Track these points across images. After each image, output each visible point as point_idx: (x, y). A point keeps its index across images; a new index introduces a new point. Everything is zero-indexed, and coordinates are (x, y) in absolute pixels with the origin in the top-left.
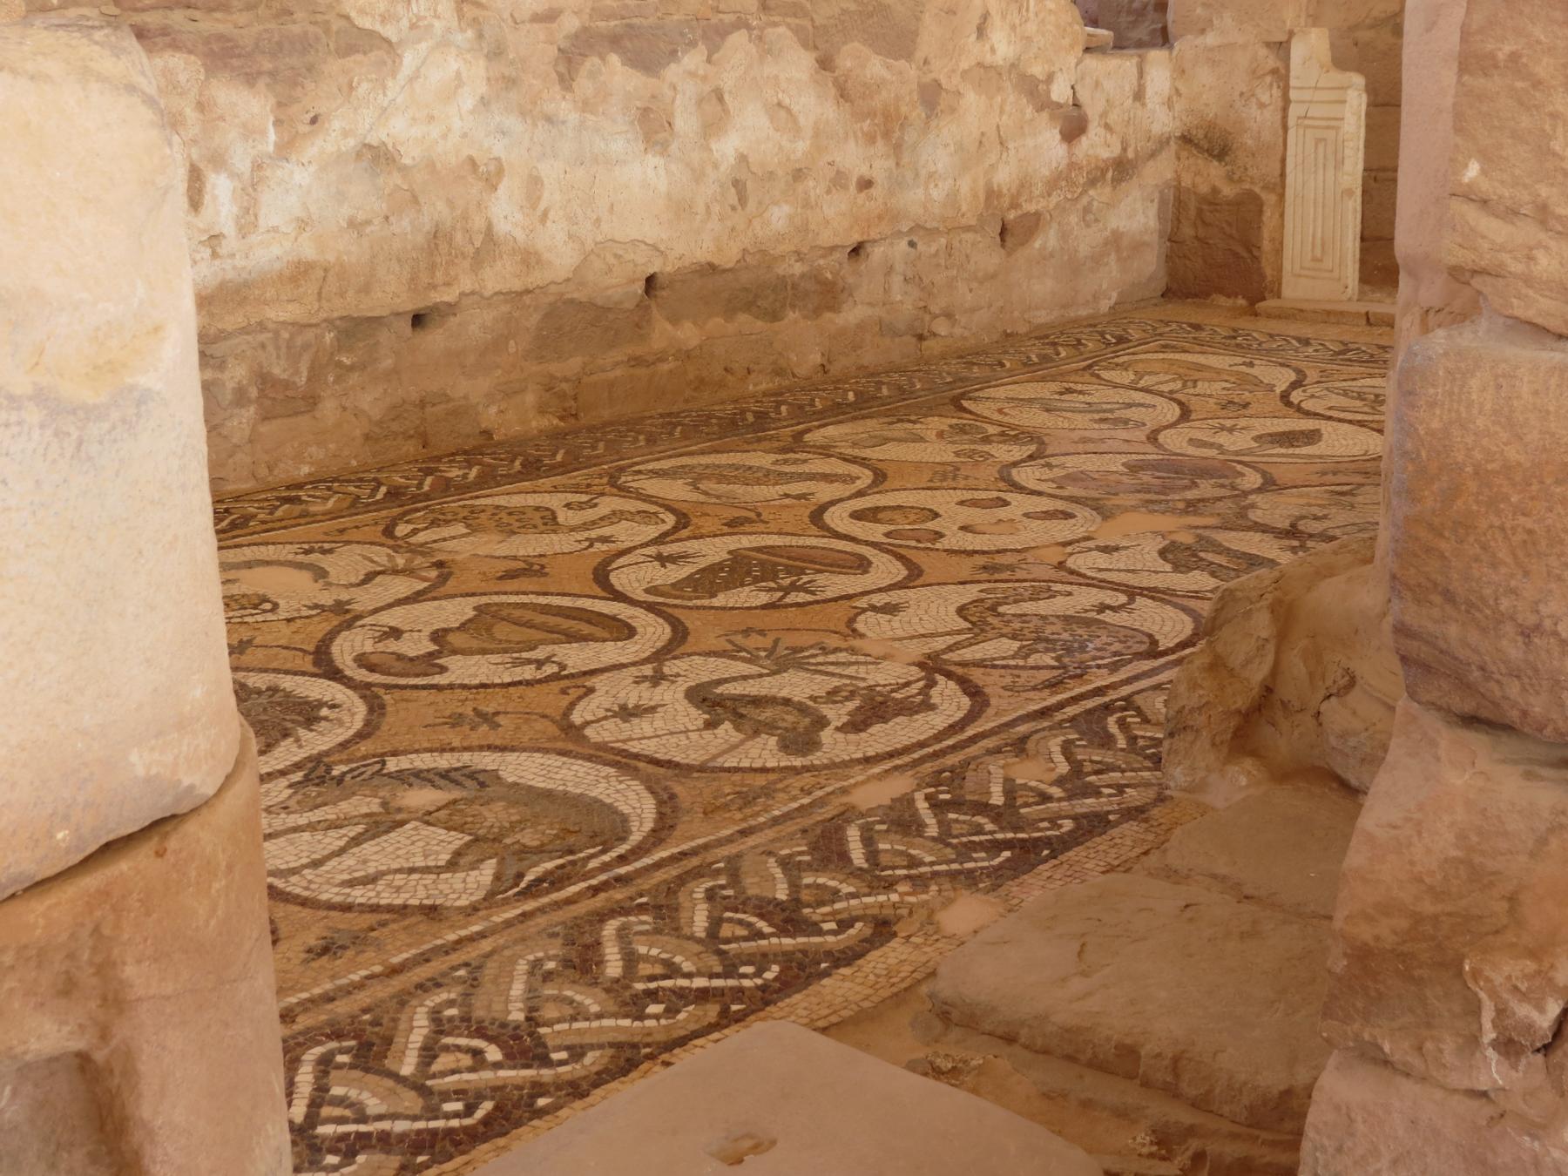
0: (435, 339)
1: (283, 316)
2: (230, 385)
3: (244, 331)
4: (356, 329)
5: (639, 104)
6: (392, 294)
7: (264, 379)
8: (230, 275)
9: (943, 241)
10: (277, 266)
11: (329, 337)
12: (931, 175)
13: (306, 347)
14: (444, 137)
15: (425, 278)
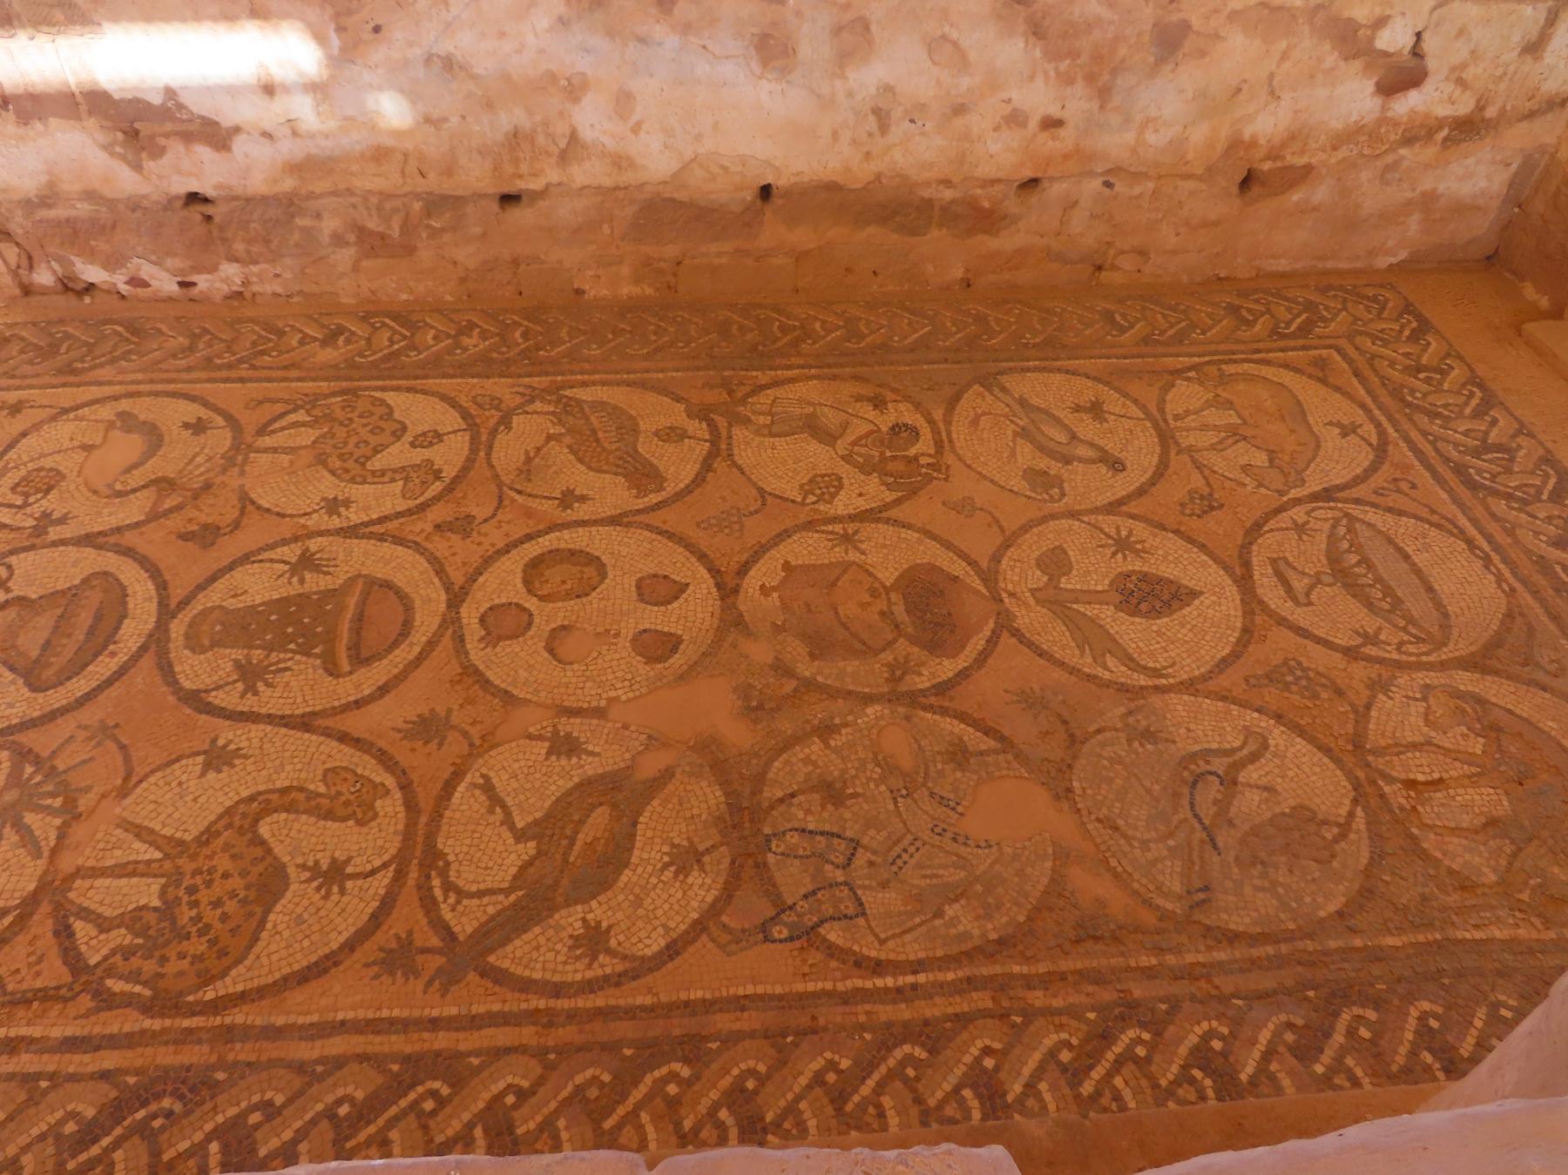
0: (520, 216)
1: (368, 185)
2: (327, 232)
3: (334, 193)
4: (436, 203)
5: (755, 30)
6: (476, 176)
7: (361, 231)
8: (314, 151)
9: (1151, 185)
10: (358, 148)
11: (417, 206)
12: (1148, 121)
13: (395, 210)
14: (519, 52)
15: (509, 169)
